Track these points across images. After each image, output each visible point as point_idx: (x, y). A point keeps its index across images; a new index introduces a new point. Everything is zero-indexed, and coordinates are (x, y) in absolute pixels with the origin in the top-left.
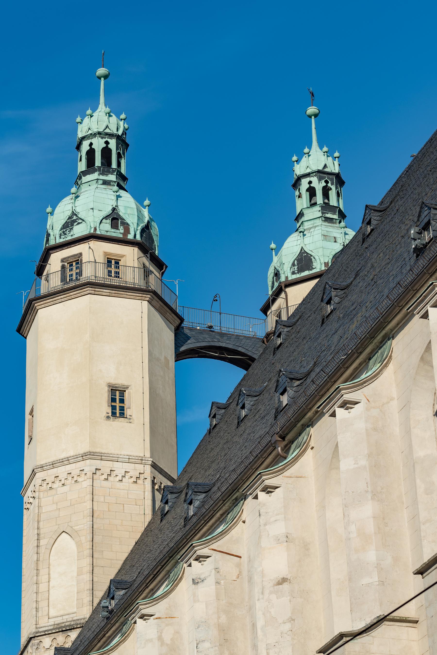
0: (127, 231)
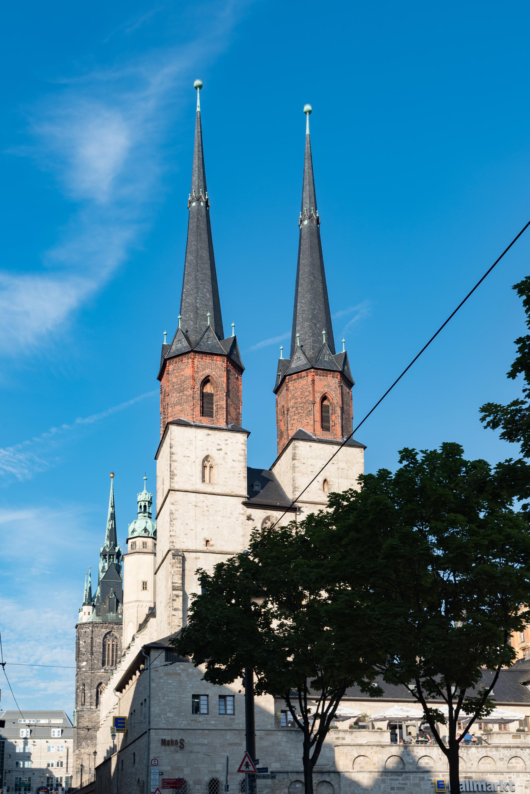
0: (149, 533)
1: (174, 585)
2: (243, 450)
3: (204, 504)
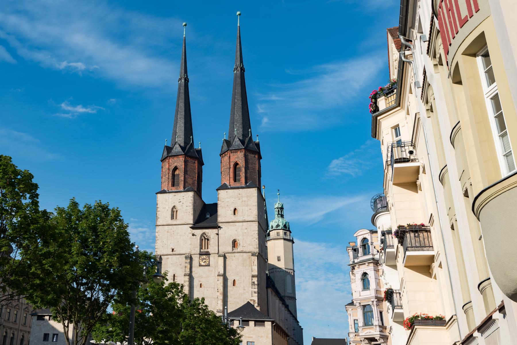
2: (191, 200)
3: (172, 231)
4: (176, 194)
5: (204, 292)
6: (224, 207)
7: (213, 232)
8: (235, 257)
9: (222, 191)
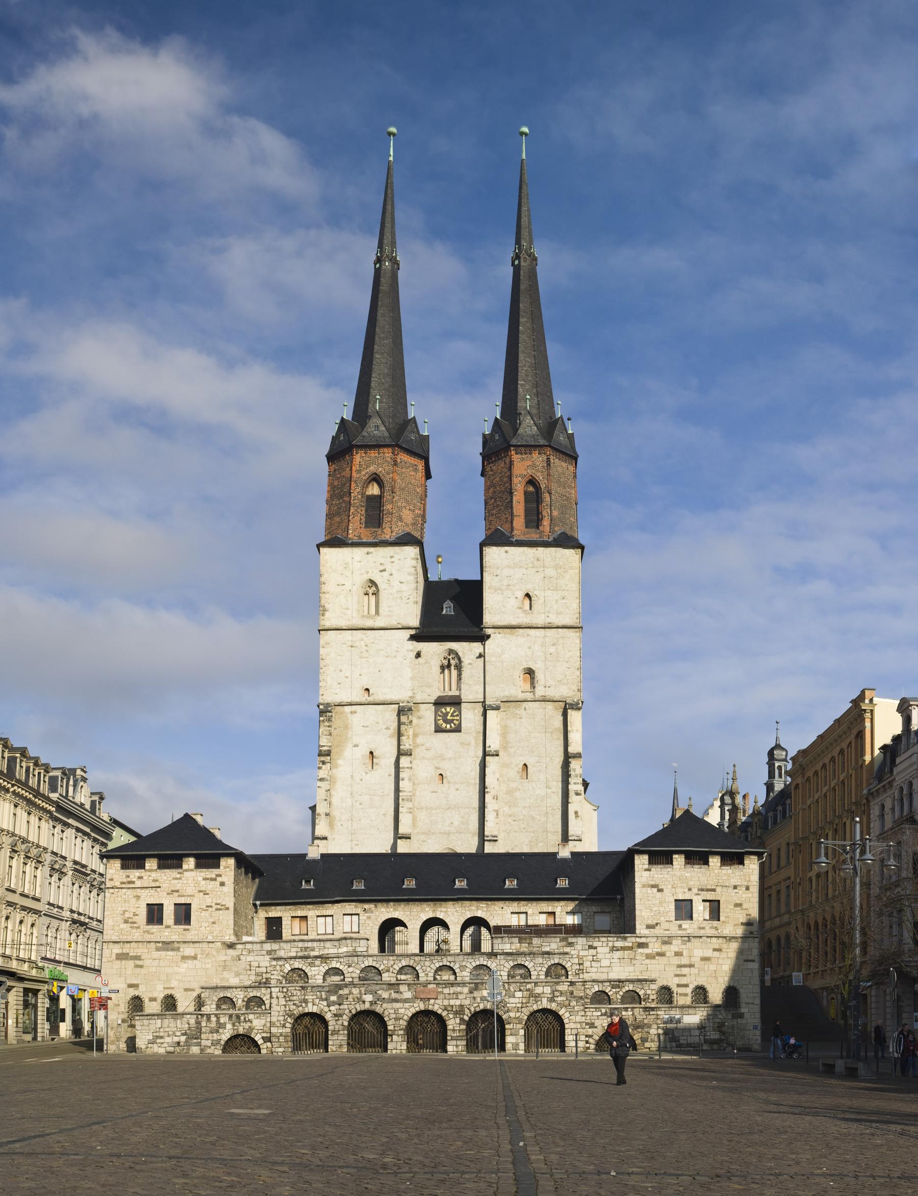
1: (321, 748)
2: (413, 567)
3: (363, 643)
4: (371, 549)
5: (448, 794)
6: (500, 589)
7: (471, 650)
8: (525, 709)
9: (494, 548)
